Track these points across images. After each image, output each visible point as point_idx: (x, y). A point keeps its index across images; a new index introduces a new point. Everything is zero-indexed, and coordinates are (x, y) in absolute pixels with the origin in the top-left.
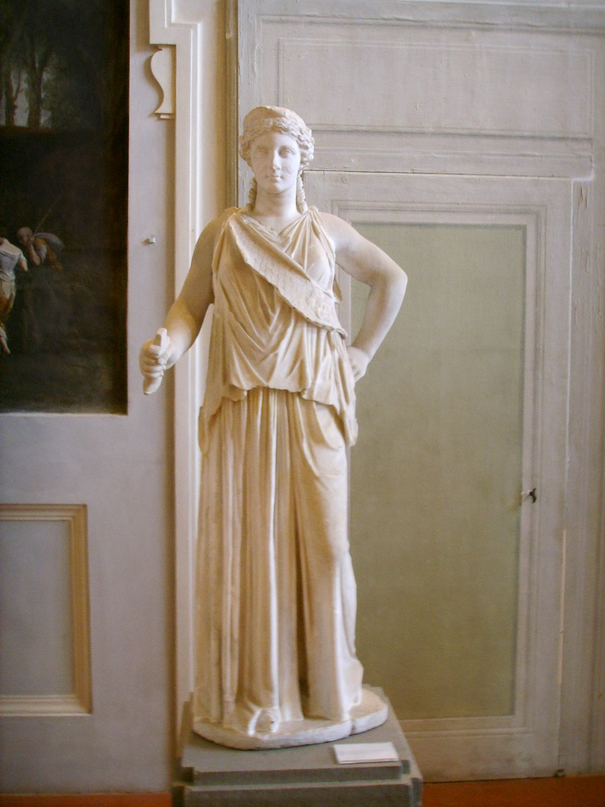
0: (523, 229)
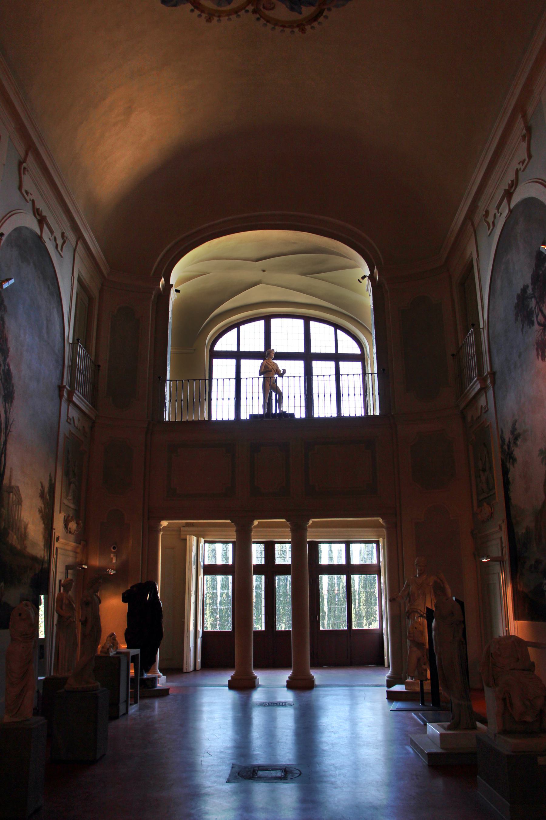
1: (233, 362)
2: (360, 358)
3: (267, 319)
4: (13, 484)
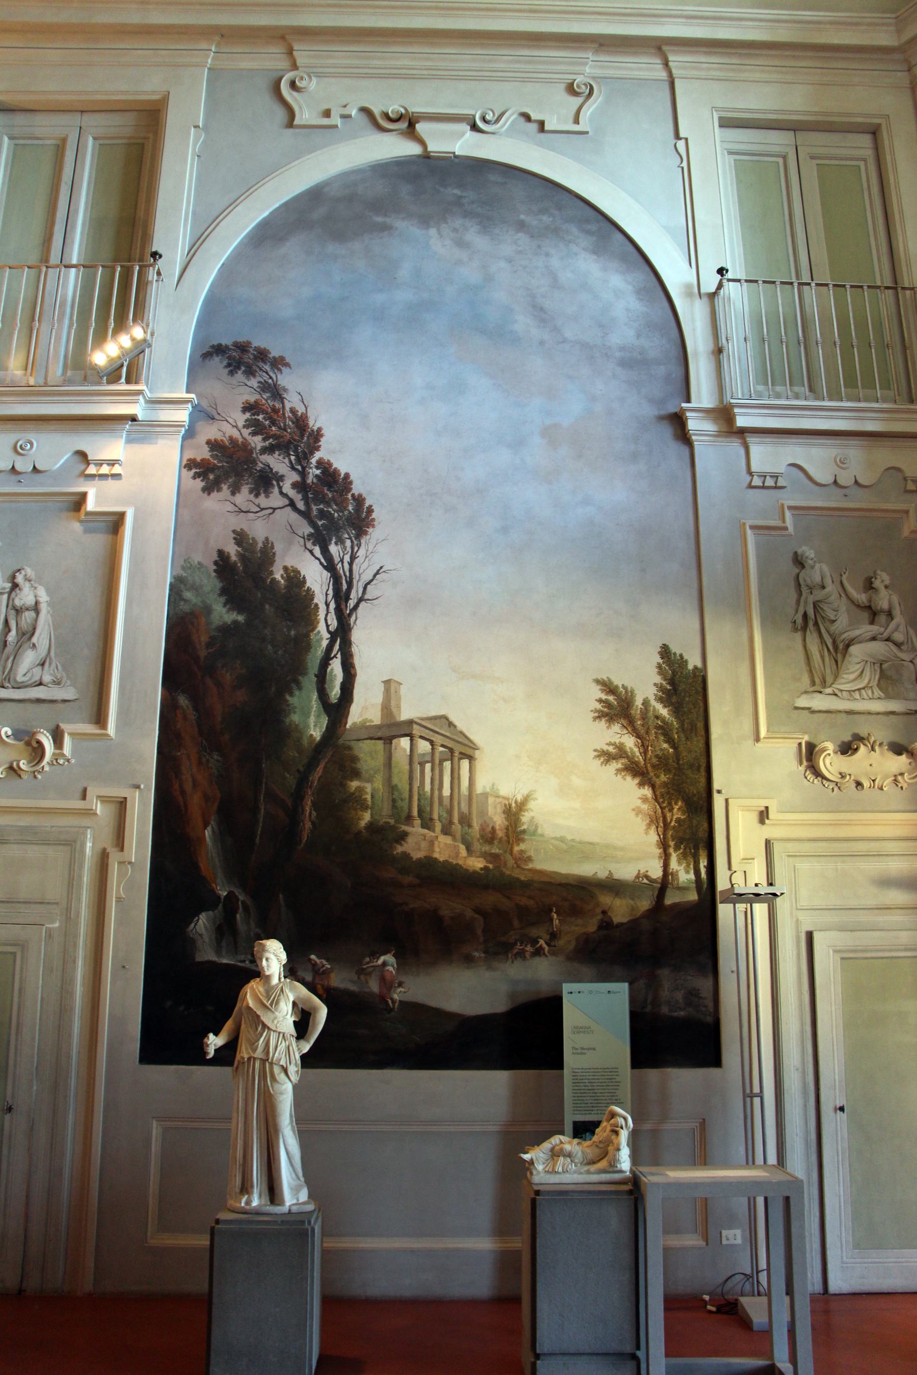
0: (14, 954)
4: (406, 713)
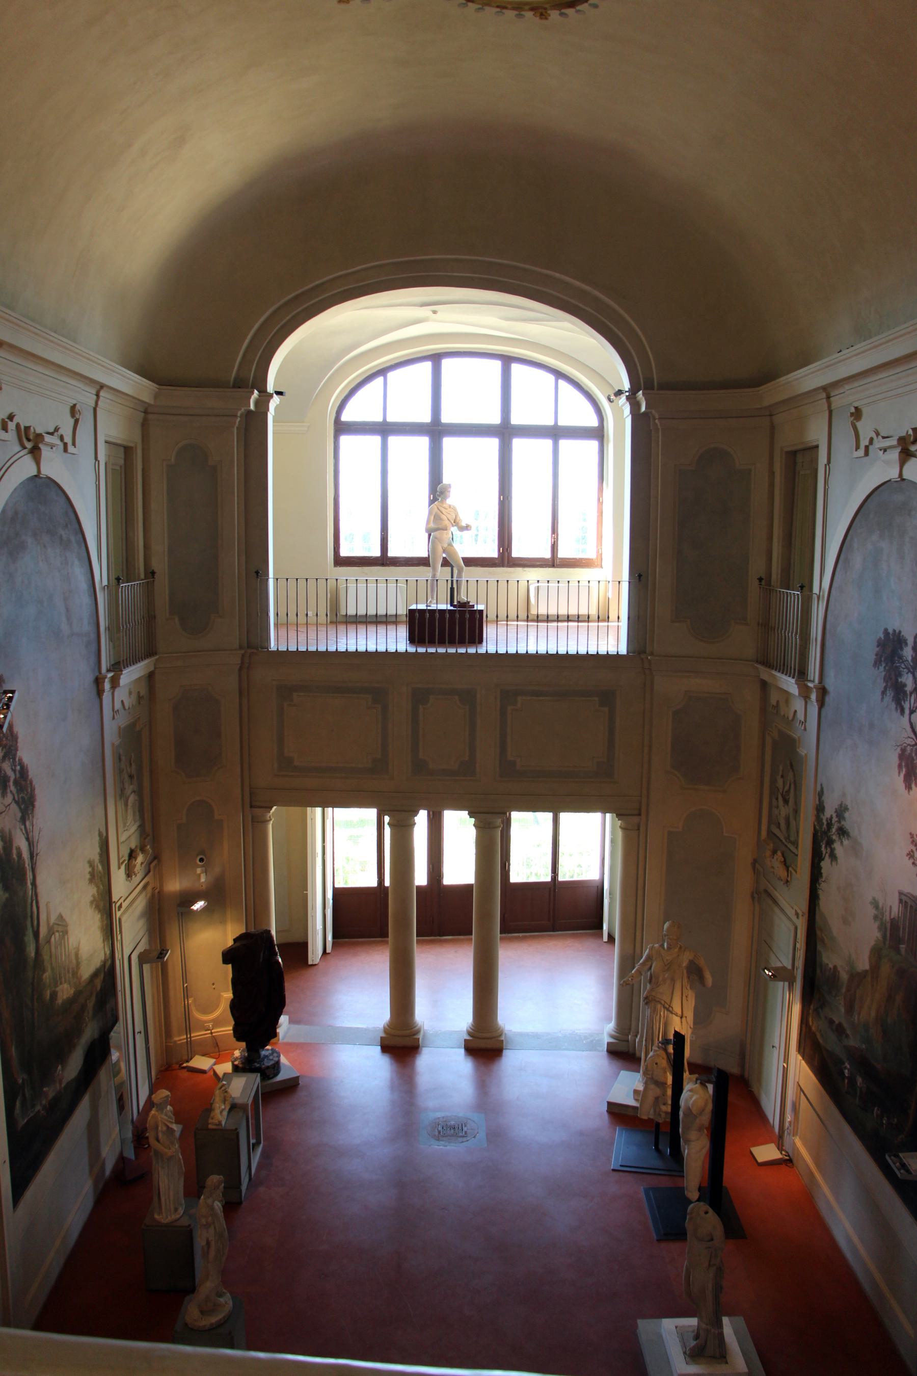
1: (376, 440)
2: (598, 434)
3: (436, 359)
